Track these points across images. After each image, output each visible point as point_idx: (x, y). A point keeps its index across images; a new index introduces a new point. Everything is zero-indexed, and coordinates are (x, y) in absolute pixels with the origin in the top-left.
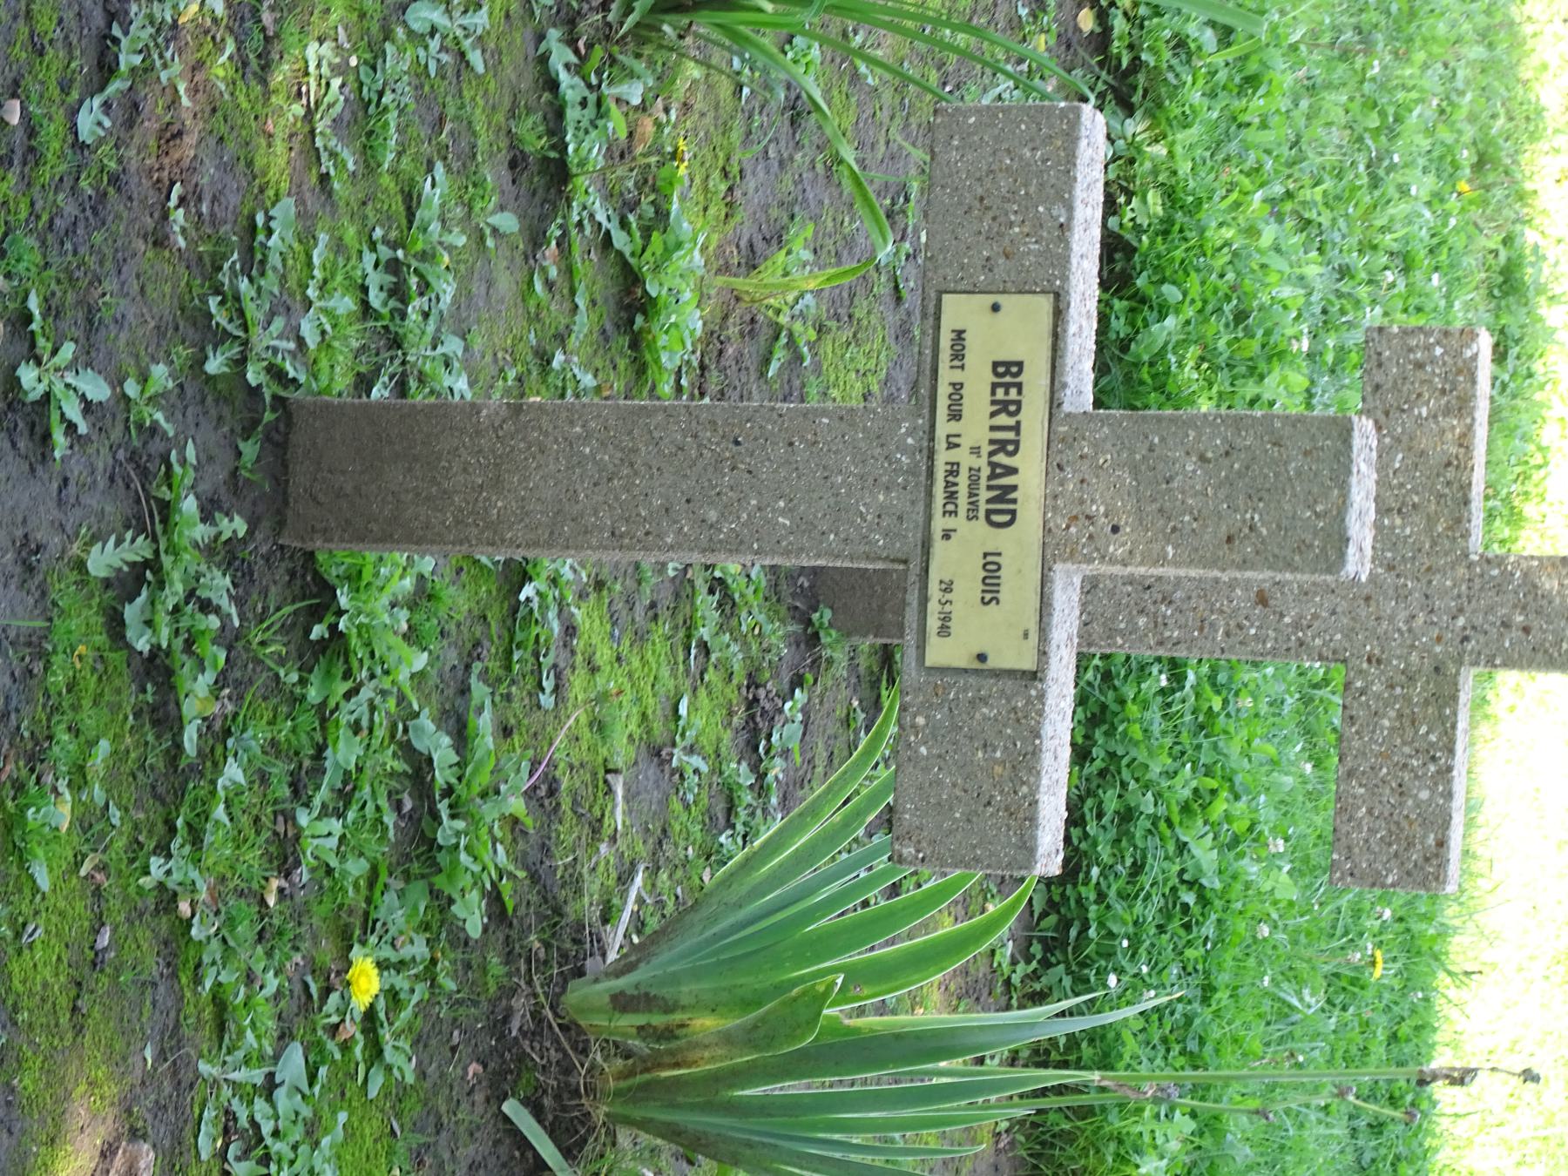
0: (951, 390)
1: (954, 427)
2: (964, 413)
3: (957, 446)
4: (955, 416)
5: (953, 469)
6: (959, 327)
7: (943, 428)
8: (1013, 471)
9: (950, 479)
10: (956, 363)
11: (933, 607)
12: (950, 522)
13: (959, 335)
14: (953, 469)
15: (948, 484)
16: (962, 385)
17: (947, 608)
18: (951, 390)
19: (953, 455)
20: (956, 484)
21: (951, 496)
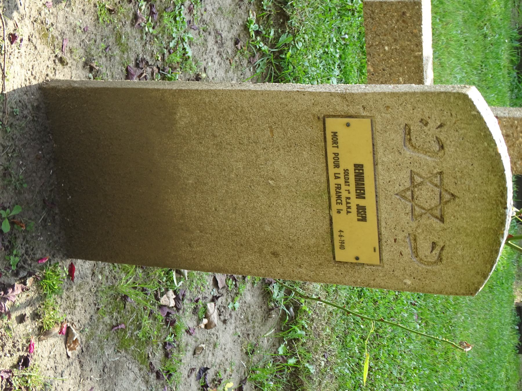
0: (334, 156)
1: (337, 170)
3: (339, 178)
4: (337, 166)
5: (338, 187)
7: (332, 171)
9: (338, 190)
10: (335, 145)
12: (339, 207)
14: (338, 187)
15: (337, 192)
16: (338, 154)
18: (334, 156)
19: (338, 181)
20: (340, 193)
21: (339, 197)
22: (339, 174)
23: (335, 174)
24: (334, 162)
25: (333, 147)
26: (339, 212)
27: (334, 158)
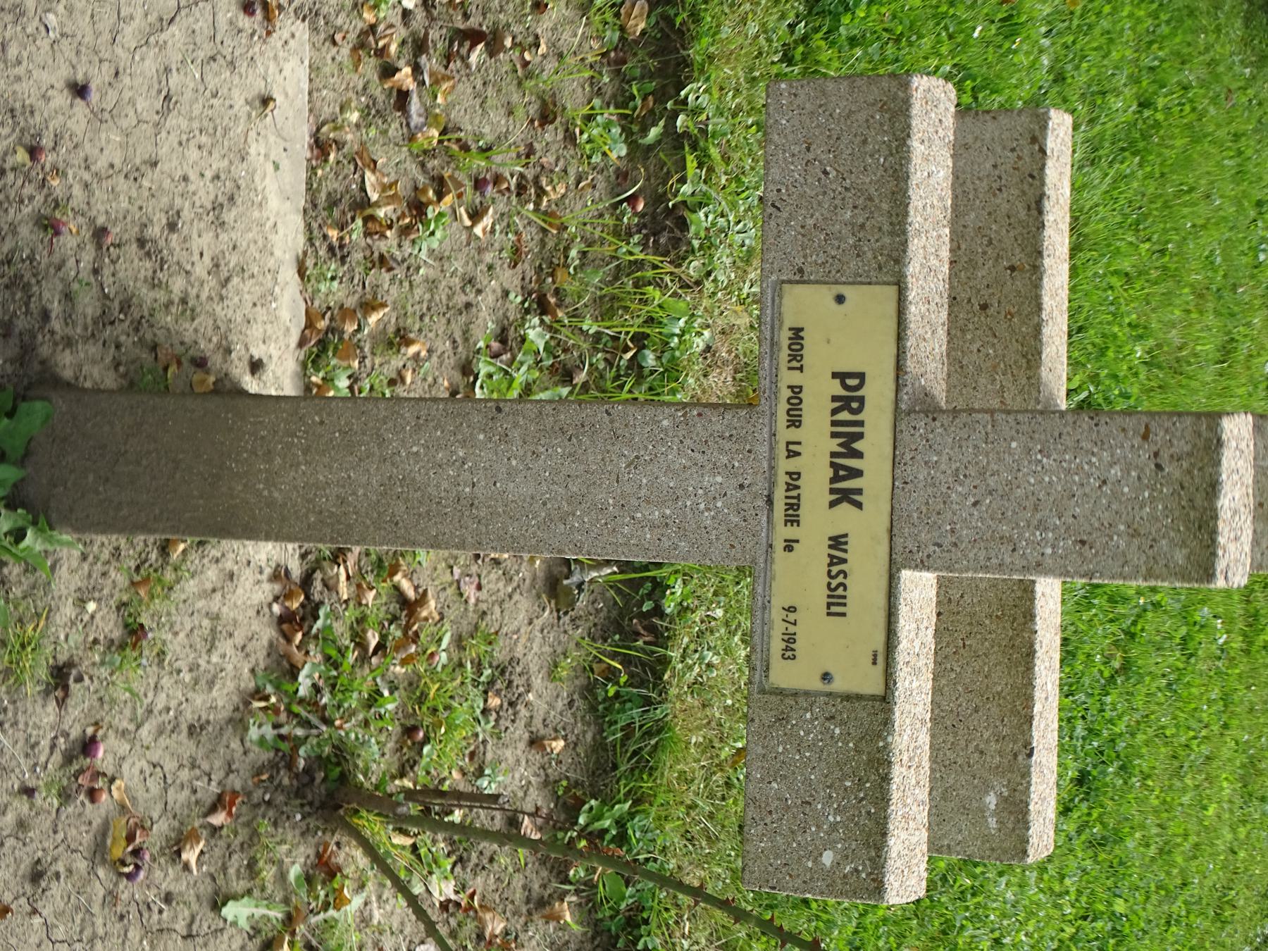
0: (789, 393)
1: (793, 434)
2: (805, 420)
3: (798, 454)
4: (795, 422)
6: (800, 326)
7: (785, 434)
8: (858, 473)
10: (795, 364)
11: (778, 629)
13: (797, 333)
16: (801, 387)
17: (792, 629)
18: (789, 393)
19: (793, 464)
21: (793, 507)
22: (799, 443)
23: (788, 443)
24: (789, 410)
25: (790, 369)
26: (788, 548)
27: (789, 399)
